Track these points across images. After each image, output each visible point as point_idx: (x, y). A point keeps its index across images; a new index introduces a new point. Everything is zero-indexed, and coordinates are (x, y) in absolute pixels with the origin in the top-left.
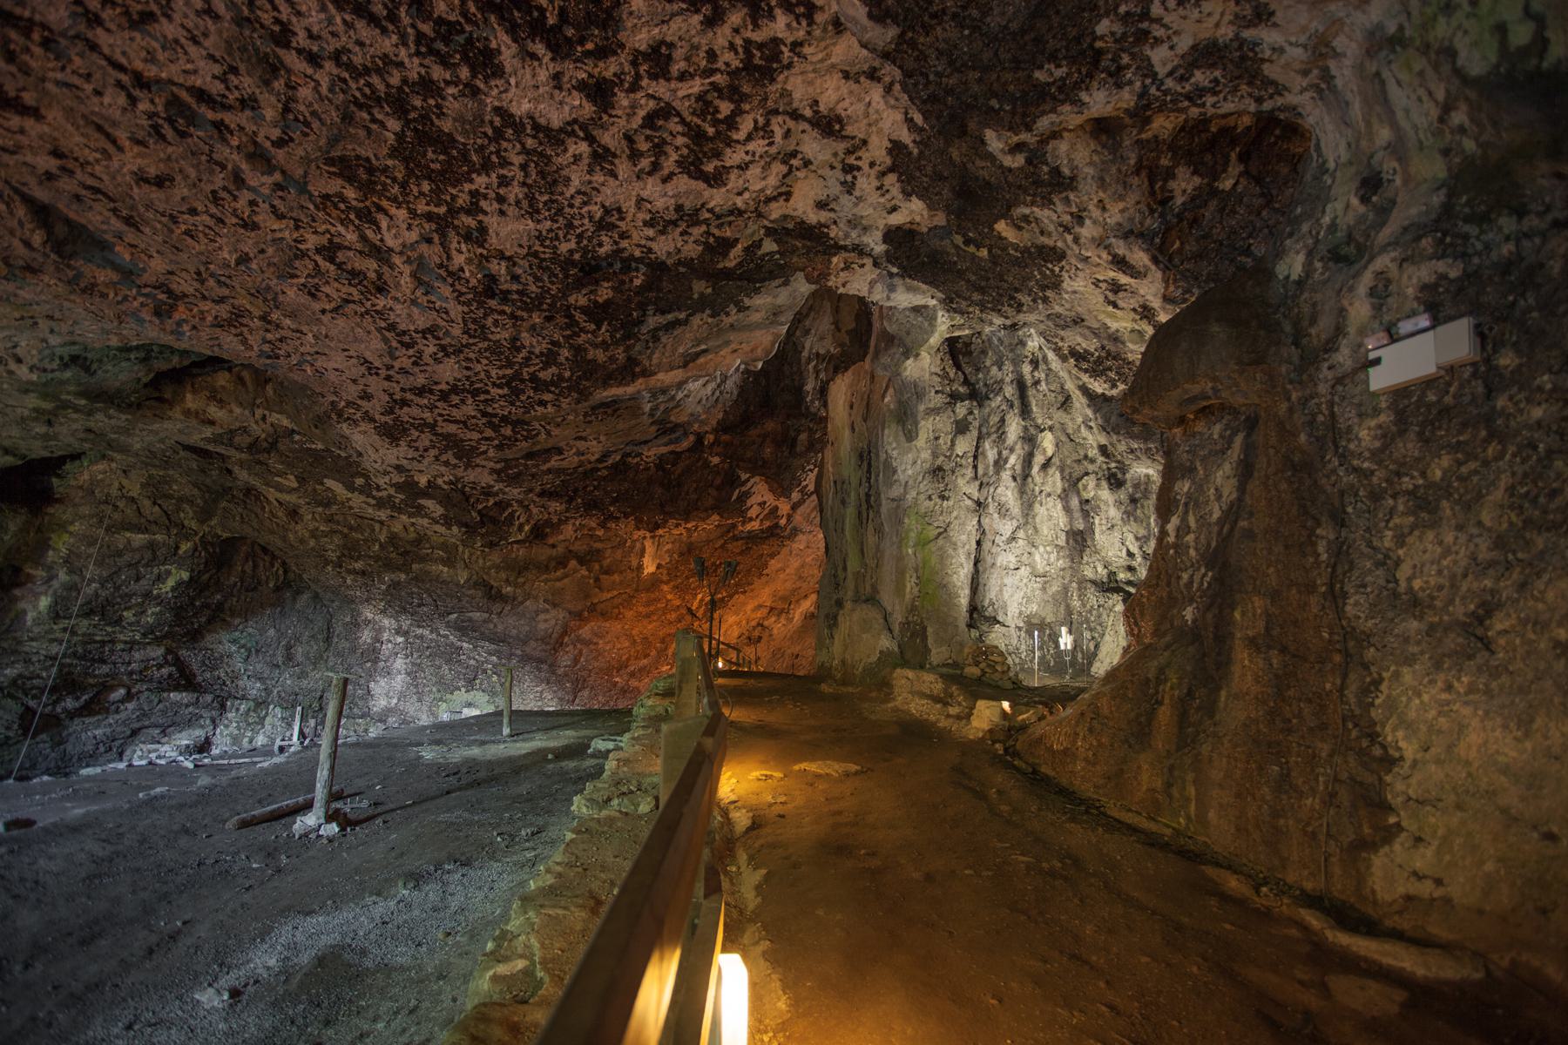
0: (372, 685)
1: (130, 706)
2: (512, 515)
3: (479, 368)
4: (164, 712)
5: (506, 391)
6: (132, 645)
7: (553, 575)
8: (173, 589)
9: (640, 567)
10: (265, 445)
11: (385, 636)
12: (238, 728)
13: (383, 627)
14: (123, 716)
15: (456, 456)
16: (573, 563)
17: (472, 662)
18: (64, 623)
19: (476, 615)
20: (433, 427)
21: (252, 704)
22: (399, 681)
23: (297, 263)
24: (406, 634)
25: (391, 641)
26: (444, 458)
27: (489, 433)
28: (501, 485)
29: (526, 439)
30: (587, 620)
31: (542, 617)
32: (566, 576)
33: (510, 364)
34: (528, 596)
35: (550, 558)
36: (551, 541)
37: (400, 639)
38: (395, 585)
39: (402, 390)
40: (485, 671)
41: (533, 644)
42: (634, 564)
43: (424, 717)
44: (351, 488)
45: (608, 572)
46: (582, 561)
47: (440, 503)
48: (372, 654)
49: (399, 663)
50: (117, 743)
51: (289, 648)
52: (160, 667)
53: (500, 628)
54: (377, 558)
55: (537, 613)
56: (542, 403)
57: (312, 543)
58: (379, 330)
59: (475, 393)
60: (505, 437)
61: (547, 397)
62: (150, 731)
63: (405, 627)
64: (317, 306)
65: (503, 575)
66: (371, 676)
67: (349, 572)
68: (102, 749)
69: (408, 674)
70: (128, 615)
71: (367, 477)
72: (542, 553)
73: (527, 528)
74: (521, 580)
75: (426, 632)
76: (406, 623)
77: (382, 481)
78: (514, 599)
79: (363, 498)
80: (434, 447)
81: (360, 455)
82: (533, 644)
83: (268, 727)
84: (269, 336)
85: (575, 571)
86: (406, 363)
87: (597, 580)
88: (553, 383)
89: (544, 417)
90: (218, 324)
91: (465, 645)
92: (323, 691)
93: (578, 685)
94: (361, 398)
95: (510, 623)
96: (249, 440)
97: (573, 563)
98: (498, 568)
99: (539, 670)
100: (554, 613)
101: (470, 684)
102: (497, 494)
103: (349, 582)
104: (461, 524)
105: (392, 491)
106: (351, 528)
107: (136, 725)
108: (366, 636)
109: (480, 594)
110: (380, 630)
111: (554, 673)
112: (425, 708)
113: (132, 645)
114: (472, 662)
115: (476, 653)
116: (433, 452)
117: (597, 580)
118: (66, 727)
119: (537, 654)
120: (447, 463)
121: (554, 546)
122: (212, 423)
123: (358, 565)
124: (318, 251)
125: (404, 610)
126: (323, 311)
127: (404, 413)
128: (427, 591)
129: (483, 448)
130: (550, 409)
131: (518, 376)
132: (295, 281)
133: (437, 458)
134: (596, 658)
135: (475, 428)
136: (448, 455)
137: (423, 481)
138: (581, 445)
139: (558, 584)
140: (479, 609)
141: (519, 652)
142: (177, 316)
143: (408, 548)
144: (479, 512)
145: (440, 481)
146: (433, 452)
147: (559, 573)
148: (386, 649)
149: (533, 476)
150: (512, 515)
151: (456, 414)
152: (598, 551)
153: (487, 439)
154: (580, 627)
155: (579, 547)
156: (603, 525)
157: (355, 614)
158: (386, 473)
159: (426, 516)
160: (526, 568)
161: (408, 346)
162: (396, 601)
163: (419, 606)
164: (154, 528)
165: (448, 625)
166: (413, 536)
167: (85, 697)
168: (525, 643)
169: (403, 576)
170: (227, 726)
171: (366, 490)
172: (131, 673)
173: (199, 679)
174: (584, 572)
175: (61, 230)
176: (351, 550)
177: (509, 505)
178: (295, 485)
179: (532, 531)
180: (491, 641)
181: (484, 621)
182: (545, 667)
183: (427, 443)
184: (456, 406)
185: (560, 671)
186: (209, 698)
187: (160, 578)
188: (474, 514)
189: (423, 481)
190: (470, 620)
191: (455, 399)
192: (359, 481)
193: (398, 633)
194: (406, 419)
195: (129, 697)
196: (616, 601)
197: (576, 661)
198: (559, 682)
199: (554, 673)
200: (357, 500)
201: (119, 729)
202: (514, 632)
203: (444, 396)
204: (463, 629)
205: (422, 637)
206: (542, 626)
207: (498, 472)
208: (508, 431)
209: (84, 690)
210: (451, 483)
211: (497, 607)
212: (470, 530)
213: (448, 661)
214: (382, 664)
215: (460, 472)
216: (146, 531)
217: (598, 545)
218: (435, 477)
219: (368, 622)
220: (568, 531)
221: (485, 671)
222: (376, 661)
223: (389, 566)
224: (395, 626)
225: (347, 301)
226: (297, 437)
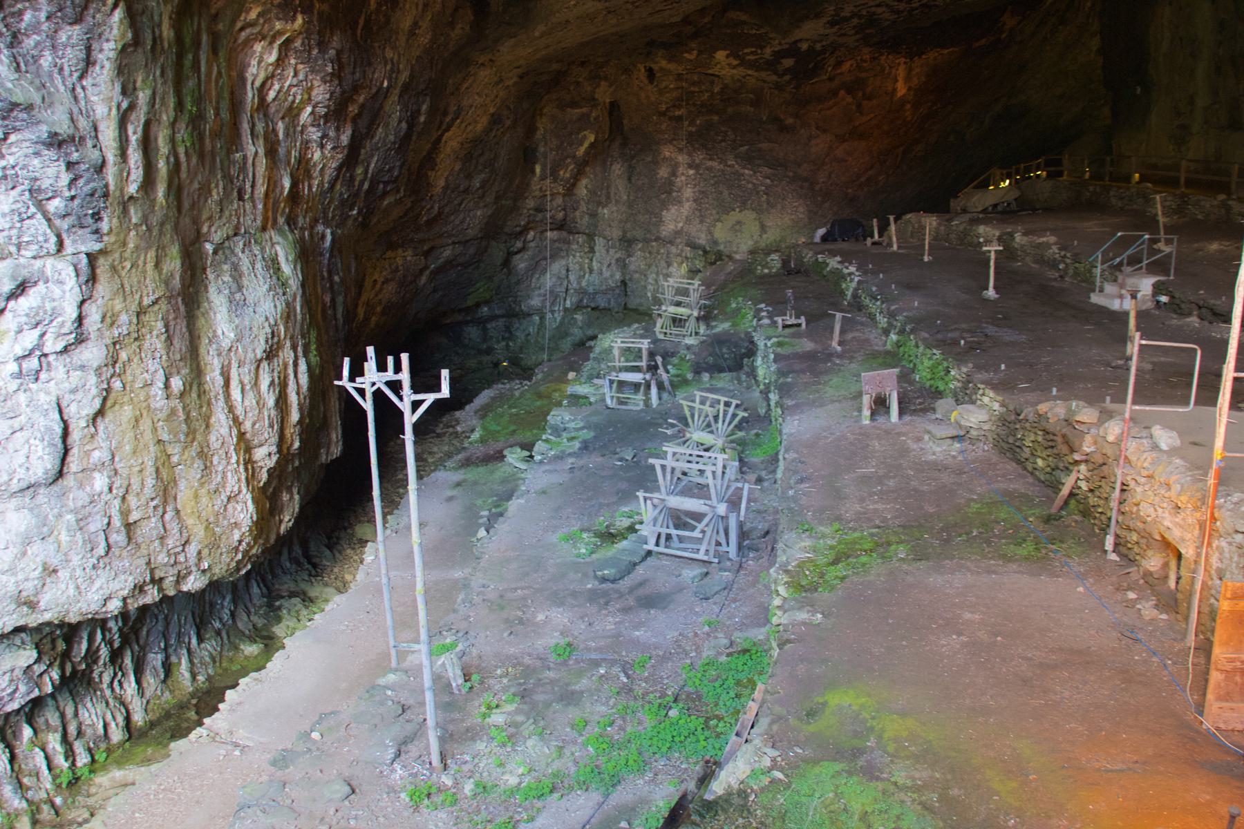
0: (664, 213)
9: (895, 90)
16: (842, 92)
17: (750, 186)
19: (764, 146)
22: (687, 207)
25: (685, 175)
31: (813, 142)
37: (691, 172)
40: (758, 193)
42: (890, 89)
43: (703, 236)
45: (869, 99)
49: (688, 192)
69: (695, 201)
75: (715, 164)
76: (699, 157)
87: (859, 106)
97: (842, 92)
99: (802, 187)
101: (743, 206)
108: (663, 172)
117: (859, 106)
162: (701, 140)
169: (716, 118)
174: (849, 99)
182: (806, 185)
185: (817, 188)
193: (690, 166)
204: (748, 160)
205: (710, 169)
217: (863, 75)
222: (669, 193)
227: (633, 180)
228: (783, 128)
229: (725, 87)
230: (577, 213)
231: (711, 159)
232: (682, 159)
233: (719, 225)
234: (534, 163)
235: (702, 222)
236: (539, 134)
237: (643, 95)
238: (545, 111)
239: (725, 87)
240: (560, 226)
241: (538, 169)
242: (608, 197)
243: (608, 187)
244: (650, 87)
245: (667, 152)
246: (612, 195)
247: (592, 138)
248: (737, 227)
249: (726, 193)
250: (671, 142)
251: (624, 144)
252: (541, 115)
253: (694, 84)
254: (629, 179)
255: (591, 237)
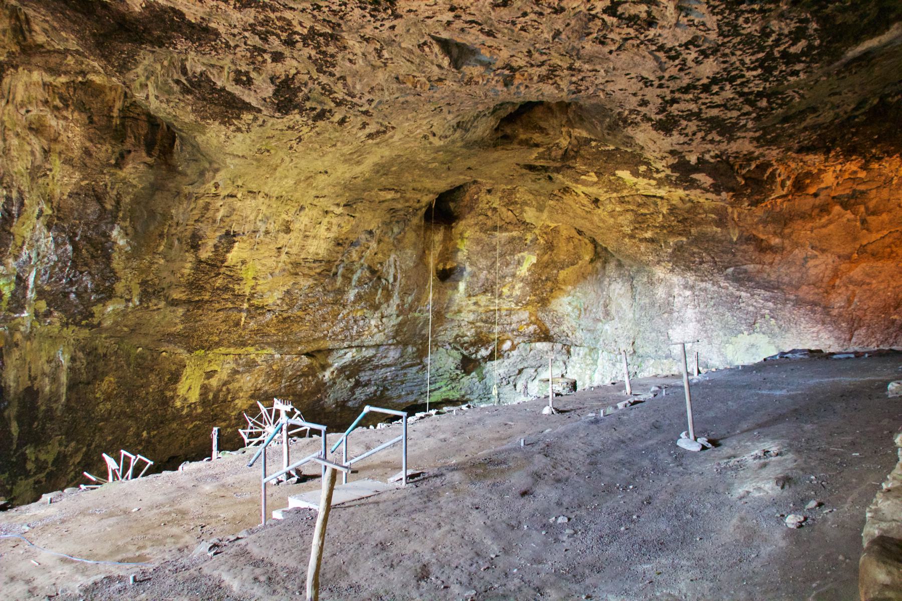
0: (670, 332)
1: (515, 353)
2: (773, 174)
3: (734, 59)
4: (534, 357)
5: (759, 71)
6: (510, 312)
7: (818, 222)
8: (529, 270)
10: (572, 153)
11: (676, 291)
12: (581, 368)
13: (672, 284)
14: (512, 360)
15: (719, 134)
17: (751, 309)
18: (474, 299)
19: (750, 267)
20: (698, 115)
21: (587, 350)
23: (591, 25)
24: (692, 288)
25: (682, 297)
26: (709, 137)
27: (747, 108)
28: (761, 150)
29: (780, 106)
30: (856, 262)
31: (811, 263)
32: (830, 222)
33: (761, 49)
34: (796, 245)
35: (814, 207)
36: (812, 190)
37: (688, 293)
38: (679, 248)
39: (672, 92)
41: (805, 288)
43: (715, 357)
44: (635, 174)
45: (874, 213)
46: (845, 206)
47: (709, 175)
48: (667, 308)
49: (690, 313)
50: (512, 378)
51: (606, 306)
52: (528, 325)
53: (773, 277)
54: (663, 227)
55: (806, 259)
56: (795, 73)
57: (612, 221)
58: (651, 53)
59: (731, 80)
60: (761, 109)
61: (798, 67)
62: (528, 370)
63: (691, 283)
64: (606, 50)
65: (770, 228)
66: (668, 324)
67: (641, 240)
68: (505, 383)
69: (698, 322)
70: (505, 291)
71: (648, 164)
72: (805, 203)
73: (788, 183)
74: (787, 231)
75: (709, 285)
76: (691, 278)
77: (659, 165)
78: (783, 249)
79: (646, 181)
80: (700, 130)
81: (642, 148)
82: (805, 288)
83: (600, 367)
84: (574, 79)
85: (840, 216)
86: (673, 71)
88: (803, 53)
89: (797, 84)
90: (542, 79)
91: (743, 294)
92: (634, 338)
93: (854, 324)
94: (640, 105)
95: (777, 271)
96: (561, 152)
97: (837, 209)
98: (765, 222)
99: (814, 312)
100: (822, 258)
102: (757, 158)
103: (643, 249)
104: (728, 190)
105: (668, 172)
106: (639, 205)
107: (520, 367)
108: (661, 292)
109: (752, 248)
110: (671, 286)
111: (828, 314)
112: (715, 350)
113: (510, 312)
114: (751, 309)
115: (754, 300)
116: (700, 135)
117: (864, 222)
118: (484, 368)
119: (810, 298)
120: (712, 141)
121: (815, 195)
122: (537, 145)
123: (649, 235)
124: (604, 11)
125: (689, 268)
126: (611, 52)
127: (674, 109)
128: (706, 250)
129: (743, 122)
130: (802, 76)
131: (770, 56)
132: (591, 37)
133: (703, 139)
134: (870, 298)
135: (735, 107)
136: (714, 135)
137: (693, 159)
138: (836, 99)
139: (824, 231)
140: (752, 261)
141: (792, 297)
142: (516, 82)
143: (686, 215)
144: (744, 177)
145: (707, 157)
146: (700, 135)
147: (824, 220)
148: (678, 302)
149: (790, 136)
150: (773, 174)
151: (717, 99)
152: (863, 193)
153: (744, 114)
154: (850, 270)
155: (844, 191)
156: (864, 167)
157: (650, 276)
158: (663, 158)
159: (699, 187)
160: (791, 220)
161: (673, 58)
162: (681, 259)
163: (701, 263)
164: (510, 227)
165: (727, 278)
166: (689, 205)
167: (491, 348)
168: (797, 288)
169: (684, 239)
170: (573, 367)
171: (648, 175)
172: (513, 330)
173: (552, 333)
174: (849, 215)
175: (455, 51)
176: (640, 221)
177: (769, 164)
178: (595, 179)
179: (794, 185)
180: (766, 288)
181: (758, 272)
183: (695, 128)
184: (717, 94)
185: (835, 312)
186: (559, 346)
187: (519, 263)
188: (739, 179)
189: (693, 159)
190: (746, 272)
191: (715, 89)
192: (642, 168)
193: (685, 288)
194: (676, 113)
195: (513, 347)
196: (888, 240)
197: (849, 301)
198: (835, 322)
199: (828, 314)
200: (642, 182)
201: (512, 369)
202: (786, 279)
203: (706, 88)
204: (741, 279)
205: (705, 290)
206: (812, 272)
207: (757, 139)
208: (764, 103)
209: (488, 342)
210: (717, 156)
211: (768, 258)
212: (738, 193)
213: (730, 309)
214: (676, 314)
215: (723, 146)
216: (506, 230)
217: (862, 187)
218: (703, 153)
219: (661, 281)
220: (829, 178)
221: (763, 316)
222: (671, 312)
223: (672, 233)
224: (682, 282)
225: (626, 40)
226: (593, 144)
227: (637, 297)
228: (763, 248)
229: (673, 209)
230: (564, 327)
231: (702, 281)
232: (676, 279)
233: (730, 348)
234: (458, 281)
235: (710, 343)
236: (461, 256)
237: (596, 219)
238: (466, 235)
239: (673, 209)
240: (545, 336)
241: (462, 286)
242: (607, 314)
243: (606, 306)
244: (600, 211)
245: (660, 272)
246: (613, 312)
247: (534, 259)
248: (754, 350)
249: (728, 314)
250: (658, 263)
251: (620, 265)
252: (462, 238)
253: (639, 205)
254: (633, 298)
255: (593, 350)
